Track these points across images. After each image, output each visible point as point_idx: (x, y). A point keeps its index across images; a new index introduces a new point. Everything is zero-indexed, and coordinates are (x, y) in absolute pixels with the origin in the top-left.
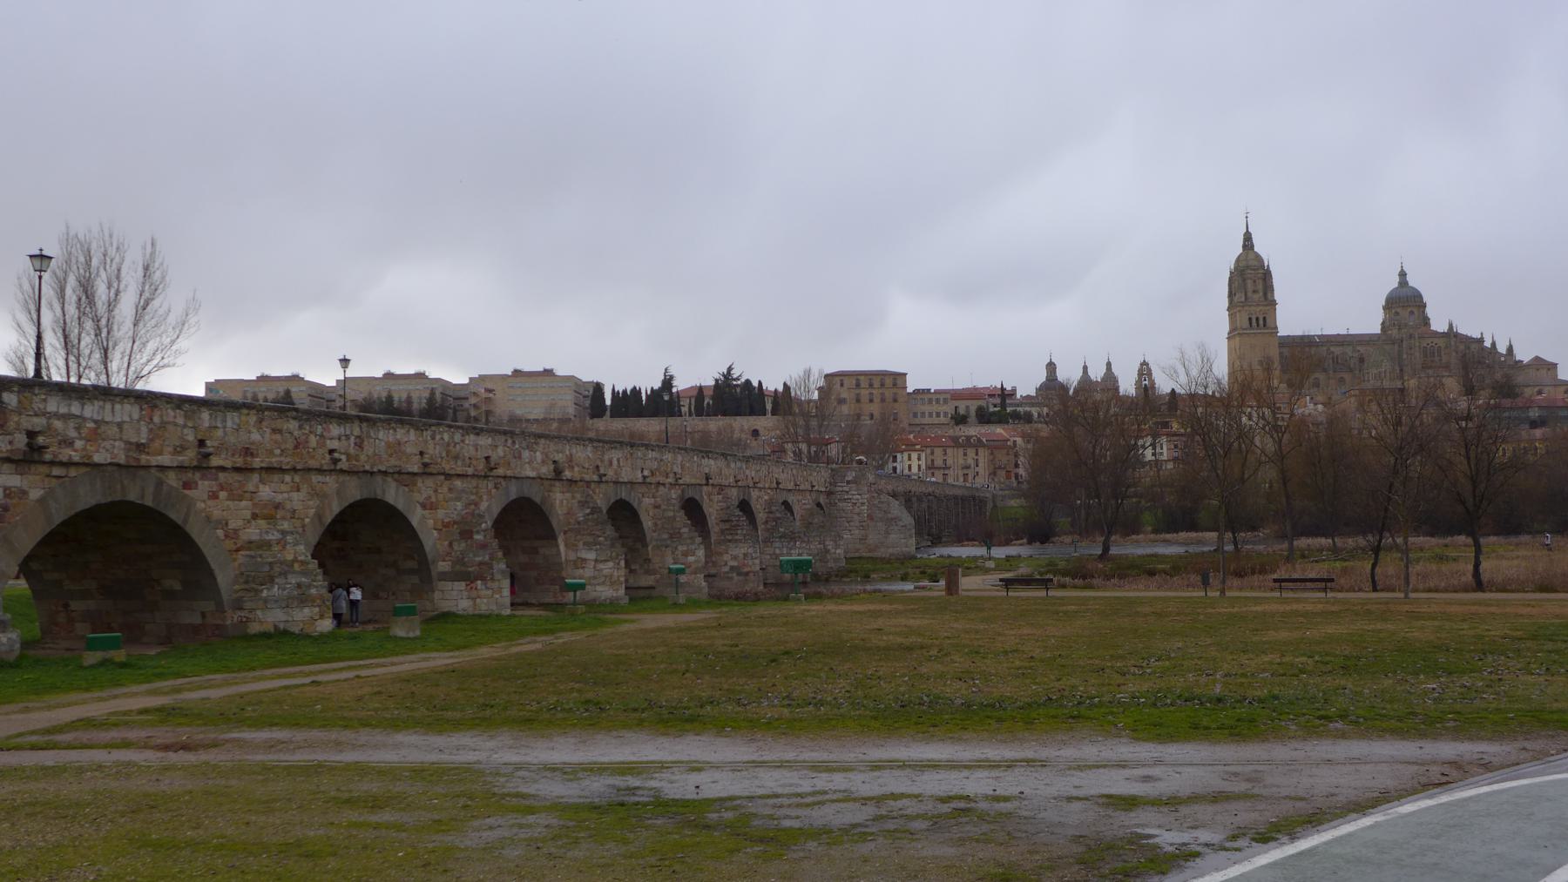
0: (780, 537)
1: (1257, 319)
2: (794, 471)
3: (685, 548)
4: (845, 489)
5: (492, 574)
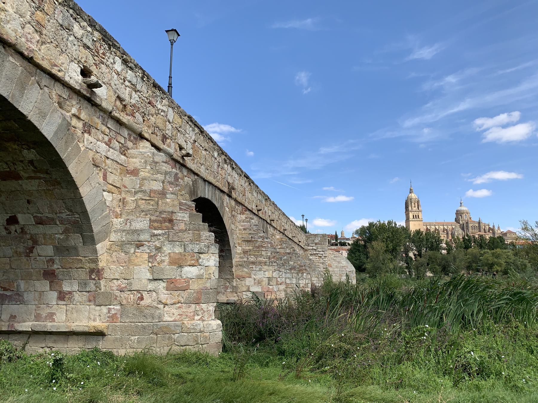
0: (291, 269)
1: (416, 216)
2: (292, 227)
3: (178, 250)
4: (314, 248)
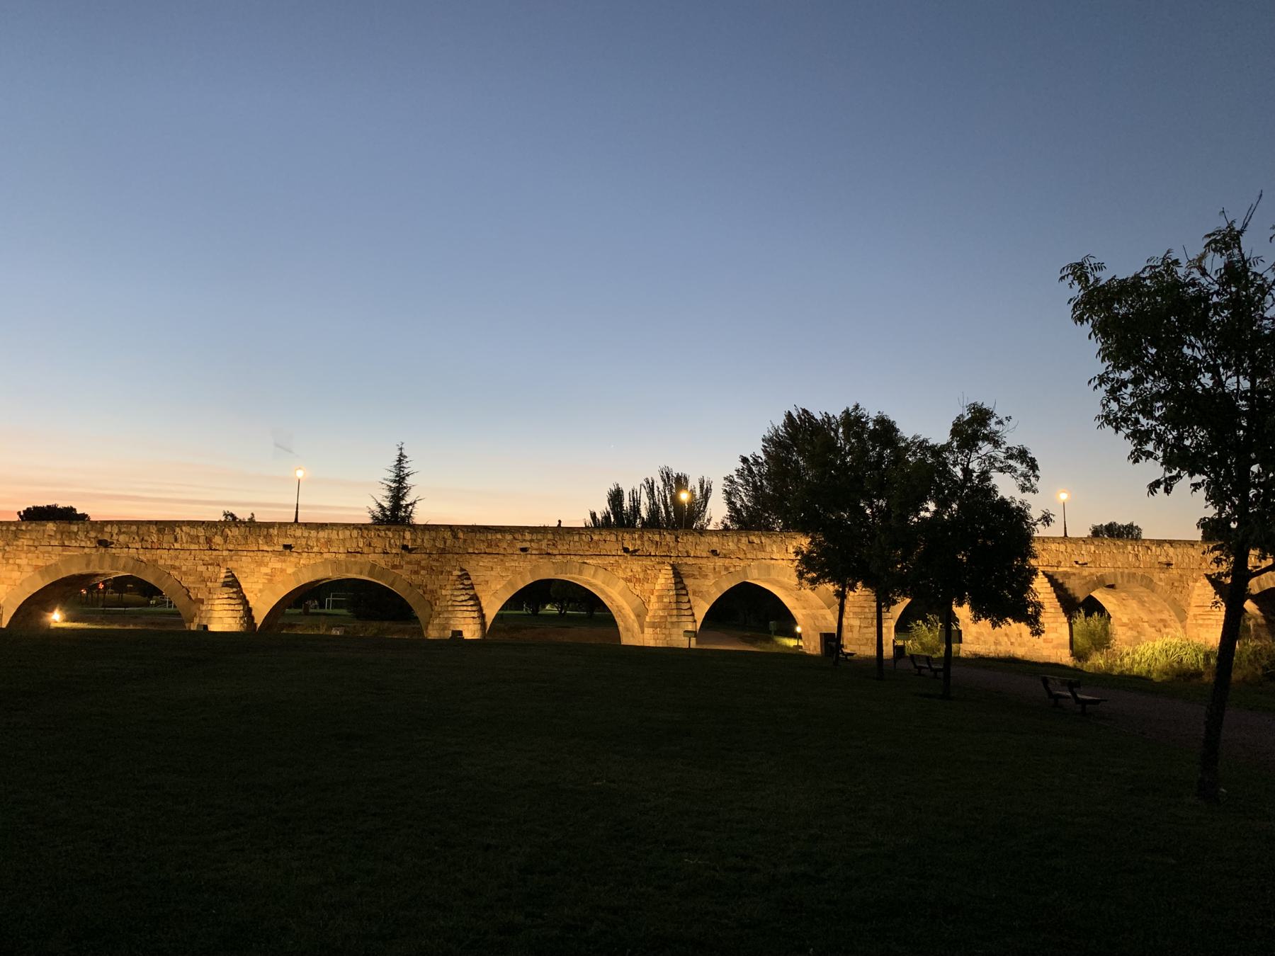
5: (665, 625)
